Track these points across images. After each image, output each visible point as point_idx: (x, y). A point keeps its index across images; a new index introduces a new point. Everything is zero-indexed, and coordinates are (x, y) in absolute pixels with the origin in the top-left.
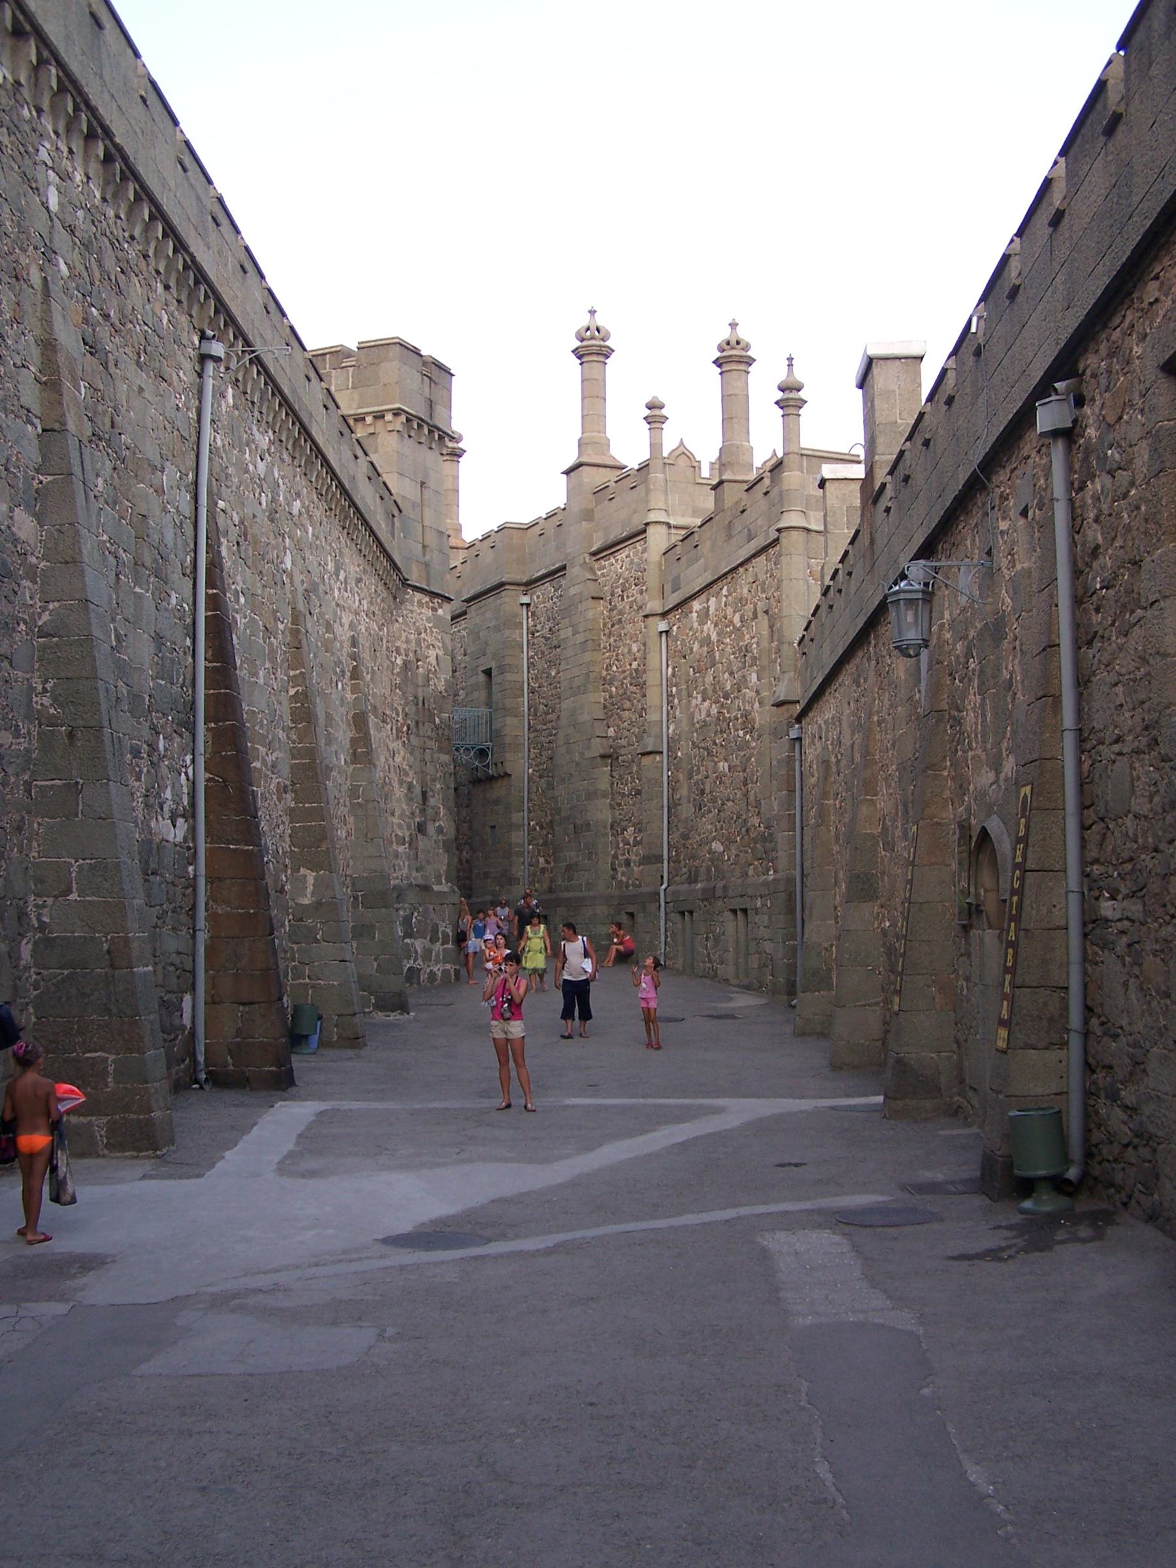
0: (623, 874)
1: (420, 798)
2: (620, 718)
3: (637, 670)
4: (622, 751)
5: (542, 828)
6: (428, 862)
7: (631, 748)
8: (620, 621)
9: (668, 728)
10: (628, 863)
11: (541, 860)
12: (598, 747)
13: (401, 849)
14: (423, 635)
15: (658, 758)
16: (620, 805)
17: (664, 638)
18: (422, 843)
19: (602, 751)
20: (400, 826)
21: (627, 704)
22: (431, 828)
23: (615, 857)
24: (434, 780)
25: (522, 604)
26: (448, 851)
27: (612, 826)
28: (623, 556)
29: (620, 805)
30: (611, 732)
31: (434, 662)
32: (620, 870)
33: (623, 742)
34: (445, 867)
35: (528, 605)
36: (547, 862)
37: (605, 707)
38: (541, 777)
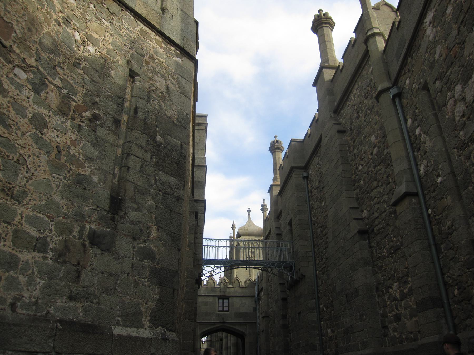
0: (395, 330)
1: (106, 205)
2: (371, 199)
3: (379, 154)
4: (376, 222)
5: (327, 307)
6: (108, 291)
7: (384, 215)
8: (359, 132)
9: (418, 170)
10: (398, 318)
11: (329, 331)
12: (355, 227)
13: (26, 256)
14: (146, 58)
15: (414, 200)
16: (382, 267)
17: (397, 101)
18: (96, 259)
19: (359, 227)
20: (33, 221)
21: (375, 183)
22: (124, 246)
23: (384, 315)
24: (144, 193)
25: (304, 178)
26: (160, 284)
27: (377, 289)
28: (355, 91)
29: (382, 267)
30: (365, 214)
31: (163, 89)
32: (391, 326)
33: (376, 215)
34: (152, 305)
35: (307, 177)
36: (333, 331)
37: (357, 199)
38: (323, 273)
